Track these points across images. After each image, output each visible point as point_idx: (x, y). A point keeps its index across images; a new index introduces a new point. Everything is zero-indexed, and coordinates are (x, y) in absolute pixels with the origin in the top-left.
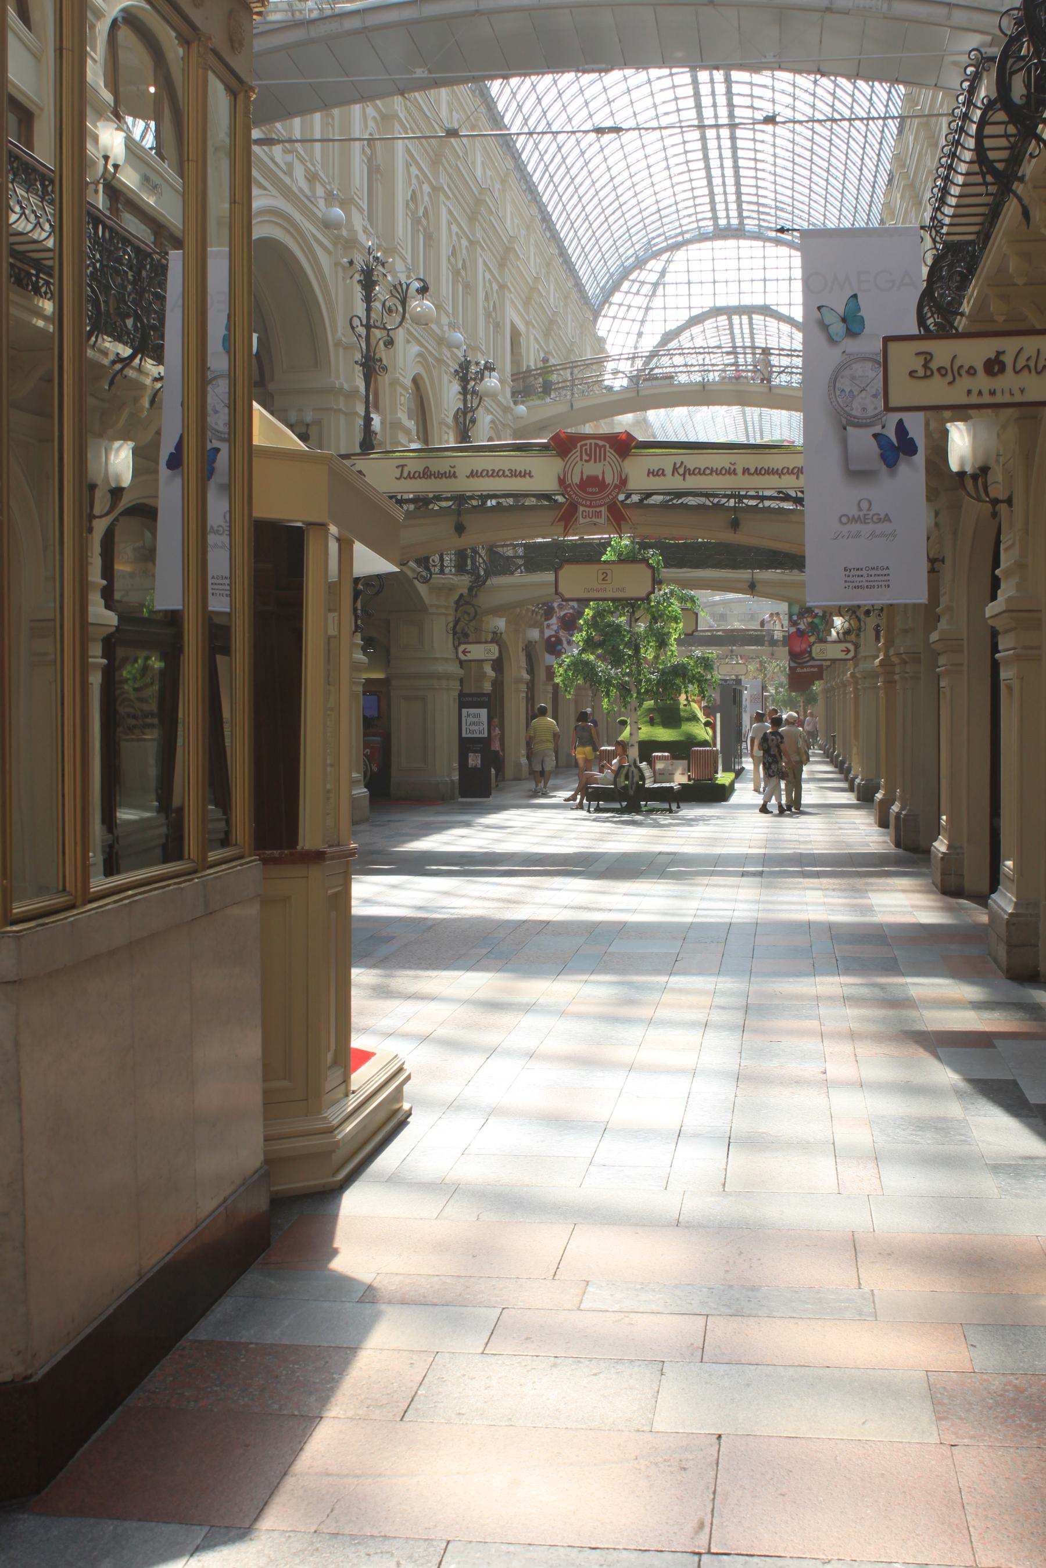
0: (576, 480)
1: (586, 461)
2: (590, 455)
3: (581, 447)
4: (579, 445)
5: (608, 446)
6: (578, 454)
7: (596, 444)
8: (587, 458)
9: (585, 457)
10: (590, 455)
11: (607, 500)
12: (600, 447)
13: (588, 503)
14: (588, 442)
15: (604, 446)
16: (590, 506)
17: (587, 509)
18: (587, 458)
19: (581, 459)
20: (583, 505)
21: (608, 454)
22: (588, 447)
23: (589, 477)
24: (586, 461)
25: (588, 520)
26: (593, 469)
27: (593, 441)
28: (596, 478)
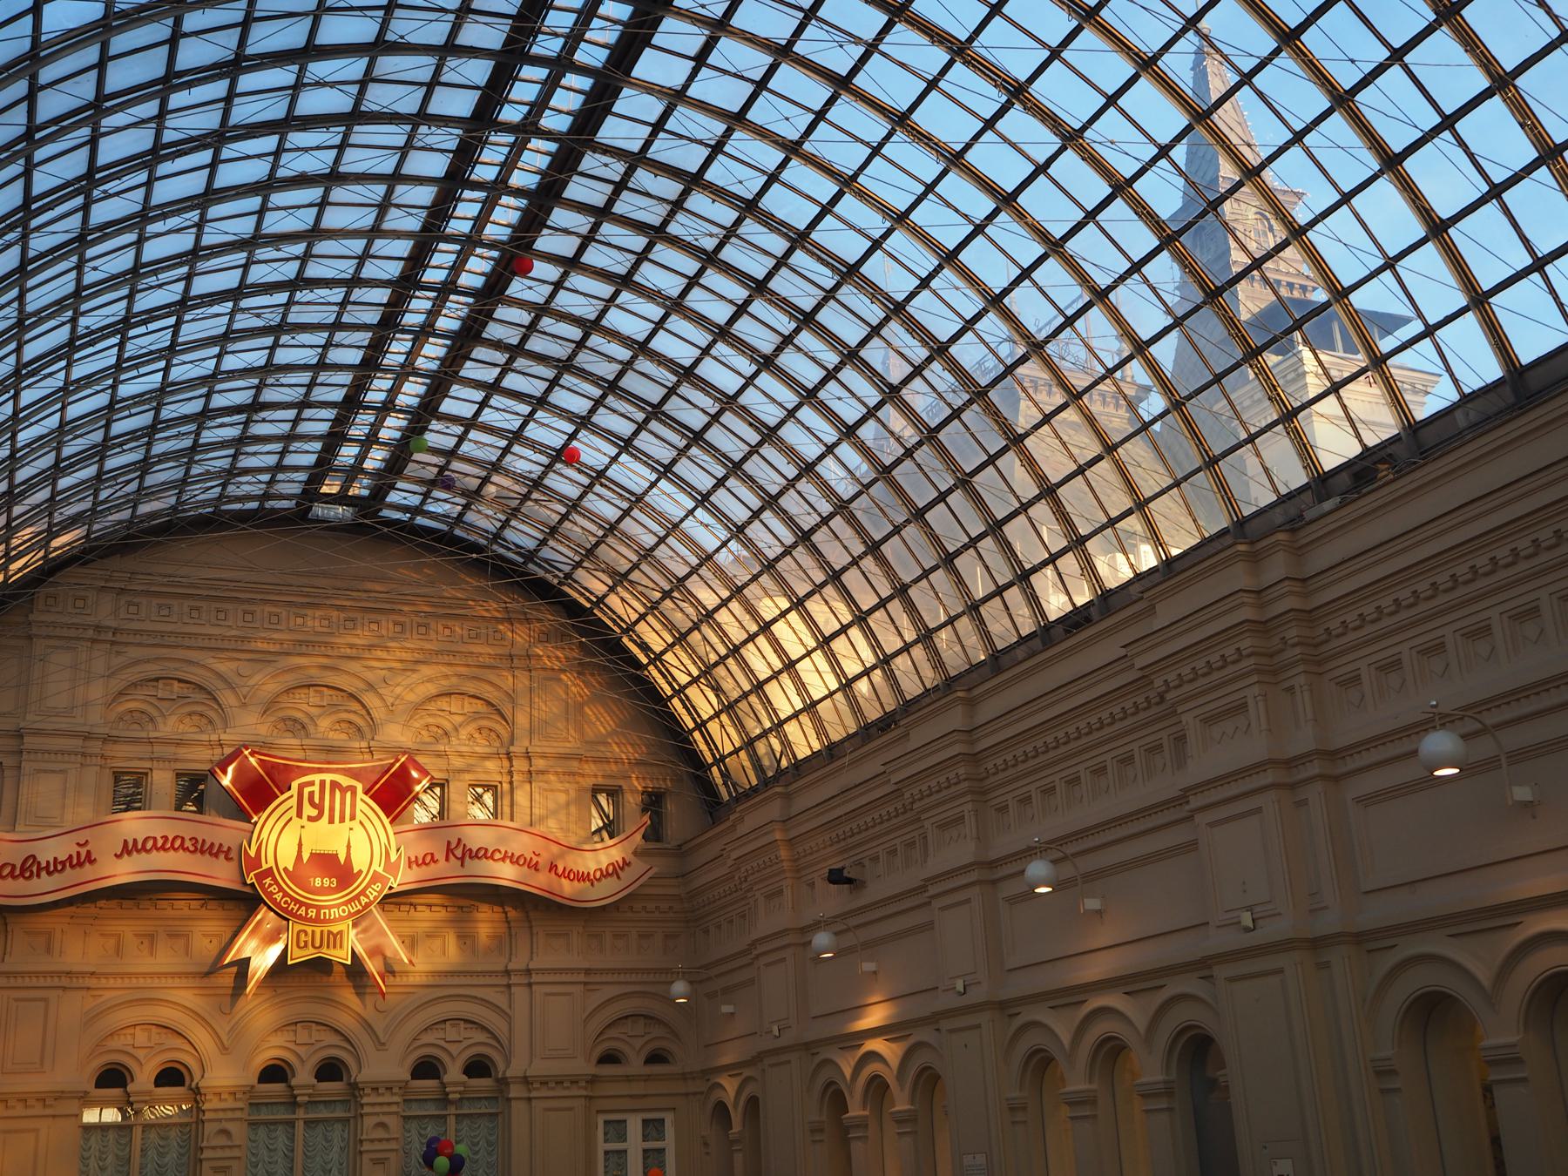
0: (287, 859)
1: (310, 819)
2: (320, 808)
4: (295, 785)
7: (334, 785)
8: (314, 813)
9: (309, 811)
10: (319, 807)
12: (344, 790)
14: (317, 778)
17: (309, 930)
18: (314, 813)
19: (300, 815)
20: (300, 917)
22: (316, 789)
23: (315, 856)
24: (310, 819)
26: (327, 837)
27: (328, 777)
28: (333, 857)
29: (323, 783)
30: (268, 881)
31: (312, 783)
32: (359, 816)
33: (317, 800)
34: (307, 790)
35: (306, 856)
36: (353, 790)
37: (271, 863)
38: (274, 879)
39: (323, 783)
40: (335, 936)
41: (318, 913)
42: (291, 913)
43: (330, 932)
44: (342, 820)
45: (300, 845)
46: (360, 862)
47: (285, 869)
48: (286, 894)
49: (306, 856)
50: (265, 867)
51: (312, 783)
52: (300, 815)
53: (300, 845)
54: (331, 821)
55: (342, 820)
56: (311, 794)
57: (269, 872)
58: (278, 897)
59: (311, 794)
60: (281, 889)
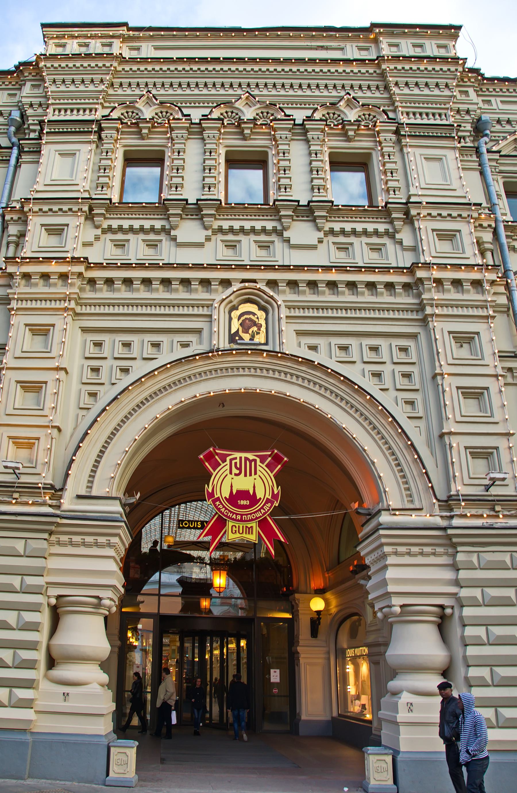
0: (226, 494)
1: (236, 475)
2: (240, 469)
3: (231, 460)
4: (228, 459)
5: (258, 460)
6: (228, 467)
7: (246, 459)
8: (237, 472)
9: (235, 471)
10: (240, 469)
11: (259, 514)
12: (251, 461)
13: (239, 517)
15: (255, 461)
16: (241, 520)
18: (237, 472)
19: (231, 473)
20: (233, 519)
21: (258, 468)
22: (238, 461)
24: (236, 475)
25: (238, 535)
26: (243, 483)
28: (248, 492)
29: (241, 458)
30: (218, 503)
31: (236, 458)
32: (258, 472)
33: (238, 466)
34: (233, 462)
35: (234, 492)
36: (255, 461)
37: (219, 495)
38: (220, 502)
39: (241, 458)
40: (249, 529)
41: (242, 518)
42: (229, 517)
43: (246, 527)
44: (250, 475)
45: (232, 486)
46: (260, 494)
47: (225, 498)
48: (226, 509)
49: (234, 492)
50: (216, 497)
51: (236, 458)
52: (231, 473)
53: (232, 486)
54: (245, 475)
55: (250, 475)
56: (236, 463)
57: (218, 499)
58: (223, 510)
59: (236, 463)
60: (224, 507)
